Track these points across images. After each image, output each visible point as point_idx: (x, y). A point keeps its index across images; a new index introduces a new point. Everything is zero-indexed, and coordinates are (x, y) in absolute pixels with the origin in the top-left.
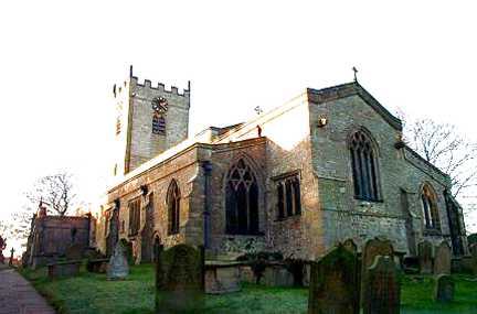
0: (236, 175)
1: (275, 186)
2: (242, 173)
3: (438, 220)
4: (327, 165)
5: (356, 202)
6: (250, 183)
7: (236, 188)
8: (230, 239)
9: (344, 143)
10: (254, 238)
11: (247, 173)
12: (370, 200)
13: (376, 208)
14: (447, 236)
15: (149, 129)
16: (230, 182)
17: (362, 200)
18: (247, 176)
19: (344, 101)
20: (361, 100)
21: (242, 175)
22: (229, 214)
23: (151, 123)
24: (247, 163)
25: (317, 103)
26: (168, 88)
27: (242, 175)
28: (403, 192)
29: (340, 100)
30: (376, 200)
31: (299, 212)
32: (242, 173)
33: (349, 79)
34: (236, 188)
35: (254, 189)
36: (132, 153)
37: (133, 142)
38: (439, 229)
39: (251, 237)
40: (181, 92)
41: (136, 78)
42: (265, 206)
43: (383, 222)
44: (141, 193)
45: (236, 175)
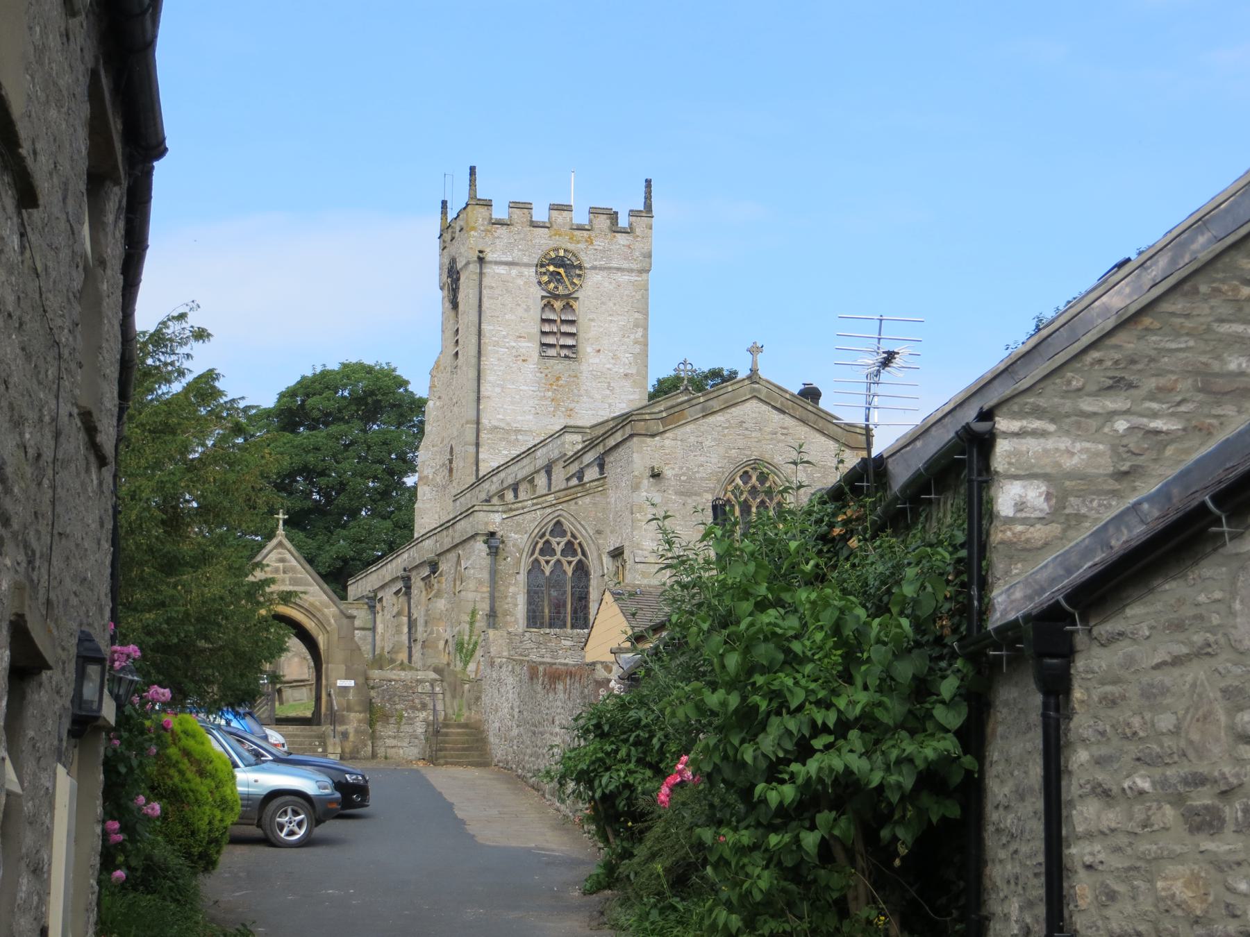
0: (547, 550)
2: (559, 544)
6: (575, 560)
7: (547, 573)
11: (569, 543)
15: (531, 348)
18: (570, 549)
19: (718, 418)
20: (765, 407)
21: (559, 549)
23: (534, 328)
24: (567, 525)
25: (653, 436)
26: (580, 217)
27: (559, 549)
29: (711, 419)
32: (559, 544)
34: (547, 573)
35: (582, 570)
36: (484, 421)
37: (486, 389)
45: (547, 550)
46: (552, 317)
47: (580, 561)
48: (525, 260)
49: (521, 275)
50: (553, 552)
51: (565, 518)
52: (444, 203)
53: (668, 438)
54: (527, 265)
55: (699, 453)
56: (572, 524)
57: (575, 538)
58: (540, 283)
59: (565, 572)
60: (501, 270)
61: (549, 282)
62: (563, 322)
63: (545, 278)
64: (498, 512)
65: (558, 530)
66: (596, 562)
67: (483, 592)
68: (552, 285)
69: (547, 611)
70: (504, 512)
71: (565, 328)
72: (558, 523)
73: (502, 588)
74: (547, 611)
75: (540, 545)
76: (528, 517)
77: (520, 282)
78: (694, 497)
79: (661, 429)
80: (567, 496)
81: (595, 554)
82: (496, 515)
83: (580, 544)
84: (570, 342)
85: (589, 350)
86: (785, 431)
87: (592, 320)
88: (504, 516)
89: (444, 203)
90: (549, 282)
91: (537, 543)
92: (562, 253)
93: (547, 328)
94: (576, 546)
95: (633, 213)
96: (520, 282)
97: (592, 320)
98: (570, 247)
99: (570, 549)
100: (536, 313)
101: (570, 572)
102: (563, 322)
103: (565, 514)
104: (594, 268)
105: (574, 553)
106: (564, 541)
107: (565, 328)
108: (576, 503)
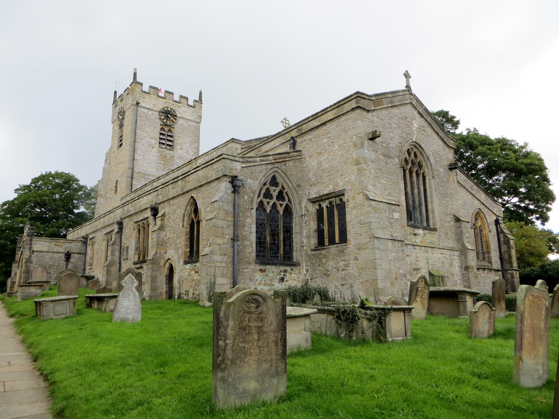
0: (268, 195)
1: (313, 209)
3: (489, 252)
4: (378, 184)
5: (410, 230)
6: (284, 203)
7: (268, 211)
8: (261, 270)
9: (397, 160)
10: (288, 269)
12: (424, 229)
13: (430, 238)
14: (498, 271)
15: (155, 142)
16: (261, 203)
17: (415, 227)
18: (280, 196)
22: (260, 242)
23: (158, 136)
24: (279, 179)
25: (368, 111)
26: (176, 98)
27: (275, 194)
28: (458, 220)
30: (428, 228)
31: (344, 239)
33: (401, 86)
34: (268, 211)
35: (288, 211)
36: (135, 169)
37: (137, 156)
38: (490, 262)
39: (283, 268)
40: (191, 103)
41: (141, 84)
42: (301, 233)
43: (436, 255)
44: (148, 213)
45: (268, 195)
46: (164, 133)
47: (287, 205)
48: (155, 108)
49: (153, 114)
50: (271, 197)
51: (278, 173)
52: (115, 92)
53: (374, 116)
54: (155, 111)
55: (389, 131)
56: (283, 178)
57: (284, 189)
58: (160, 119)
59: (278, 212)
60: (145, 111)
61: (164, 119)
62: (168, 135)
63: (163, 117)
64: (239, 161)
65: (274, 182)
66: (297, 206)
67: (229, 221)
68: (165, 120)
69: (268, 238)
70: (243, 162)
71: (169, 138)
72: (274, 178)
73: (242, 219)
74: (268, 238)
75: (263, 191)
76: (258, 169)
77: (153, 117)
78: (391, 160)
79: (373, 108)
80: (280, 158)
81: (297, 201)
82: (238, 164)
83: (286, 193)
84: (170, 143)
85: (178, 148)
86: (423, 129)
87: (180, 137)
88: (243, 165)
89: (115, 92)
90: (164, 119)
91: (261, 189)
92: (169, 109)
93: (162, 137)
94: (285, 194)
95: (195, 101)
96: (153, 117)
97: (180, 137)
98: (172, 107)
99: (280, 196)
100: (158, 130)
101: (281, 213)
102: (168, 135)
103: (279, 171)
104: (181, 117)
105: (283, 200)
106: (278, 190)
107: (169, 138)
108: (285, 165)
